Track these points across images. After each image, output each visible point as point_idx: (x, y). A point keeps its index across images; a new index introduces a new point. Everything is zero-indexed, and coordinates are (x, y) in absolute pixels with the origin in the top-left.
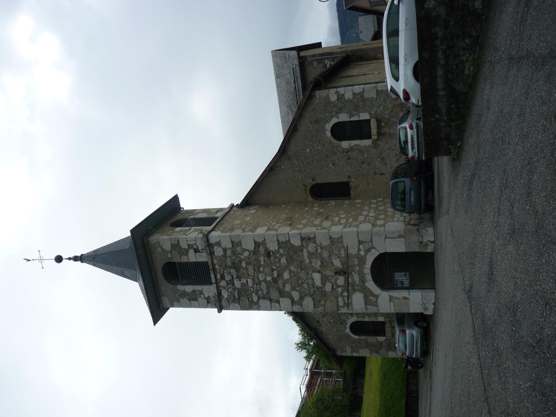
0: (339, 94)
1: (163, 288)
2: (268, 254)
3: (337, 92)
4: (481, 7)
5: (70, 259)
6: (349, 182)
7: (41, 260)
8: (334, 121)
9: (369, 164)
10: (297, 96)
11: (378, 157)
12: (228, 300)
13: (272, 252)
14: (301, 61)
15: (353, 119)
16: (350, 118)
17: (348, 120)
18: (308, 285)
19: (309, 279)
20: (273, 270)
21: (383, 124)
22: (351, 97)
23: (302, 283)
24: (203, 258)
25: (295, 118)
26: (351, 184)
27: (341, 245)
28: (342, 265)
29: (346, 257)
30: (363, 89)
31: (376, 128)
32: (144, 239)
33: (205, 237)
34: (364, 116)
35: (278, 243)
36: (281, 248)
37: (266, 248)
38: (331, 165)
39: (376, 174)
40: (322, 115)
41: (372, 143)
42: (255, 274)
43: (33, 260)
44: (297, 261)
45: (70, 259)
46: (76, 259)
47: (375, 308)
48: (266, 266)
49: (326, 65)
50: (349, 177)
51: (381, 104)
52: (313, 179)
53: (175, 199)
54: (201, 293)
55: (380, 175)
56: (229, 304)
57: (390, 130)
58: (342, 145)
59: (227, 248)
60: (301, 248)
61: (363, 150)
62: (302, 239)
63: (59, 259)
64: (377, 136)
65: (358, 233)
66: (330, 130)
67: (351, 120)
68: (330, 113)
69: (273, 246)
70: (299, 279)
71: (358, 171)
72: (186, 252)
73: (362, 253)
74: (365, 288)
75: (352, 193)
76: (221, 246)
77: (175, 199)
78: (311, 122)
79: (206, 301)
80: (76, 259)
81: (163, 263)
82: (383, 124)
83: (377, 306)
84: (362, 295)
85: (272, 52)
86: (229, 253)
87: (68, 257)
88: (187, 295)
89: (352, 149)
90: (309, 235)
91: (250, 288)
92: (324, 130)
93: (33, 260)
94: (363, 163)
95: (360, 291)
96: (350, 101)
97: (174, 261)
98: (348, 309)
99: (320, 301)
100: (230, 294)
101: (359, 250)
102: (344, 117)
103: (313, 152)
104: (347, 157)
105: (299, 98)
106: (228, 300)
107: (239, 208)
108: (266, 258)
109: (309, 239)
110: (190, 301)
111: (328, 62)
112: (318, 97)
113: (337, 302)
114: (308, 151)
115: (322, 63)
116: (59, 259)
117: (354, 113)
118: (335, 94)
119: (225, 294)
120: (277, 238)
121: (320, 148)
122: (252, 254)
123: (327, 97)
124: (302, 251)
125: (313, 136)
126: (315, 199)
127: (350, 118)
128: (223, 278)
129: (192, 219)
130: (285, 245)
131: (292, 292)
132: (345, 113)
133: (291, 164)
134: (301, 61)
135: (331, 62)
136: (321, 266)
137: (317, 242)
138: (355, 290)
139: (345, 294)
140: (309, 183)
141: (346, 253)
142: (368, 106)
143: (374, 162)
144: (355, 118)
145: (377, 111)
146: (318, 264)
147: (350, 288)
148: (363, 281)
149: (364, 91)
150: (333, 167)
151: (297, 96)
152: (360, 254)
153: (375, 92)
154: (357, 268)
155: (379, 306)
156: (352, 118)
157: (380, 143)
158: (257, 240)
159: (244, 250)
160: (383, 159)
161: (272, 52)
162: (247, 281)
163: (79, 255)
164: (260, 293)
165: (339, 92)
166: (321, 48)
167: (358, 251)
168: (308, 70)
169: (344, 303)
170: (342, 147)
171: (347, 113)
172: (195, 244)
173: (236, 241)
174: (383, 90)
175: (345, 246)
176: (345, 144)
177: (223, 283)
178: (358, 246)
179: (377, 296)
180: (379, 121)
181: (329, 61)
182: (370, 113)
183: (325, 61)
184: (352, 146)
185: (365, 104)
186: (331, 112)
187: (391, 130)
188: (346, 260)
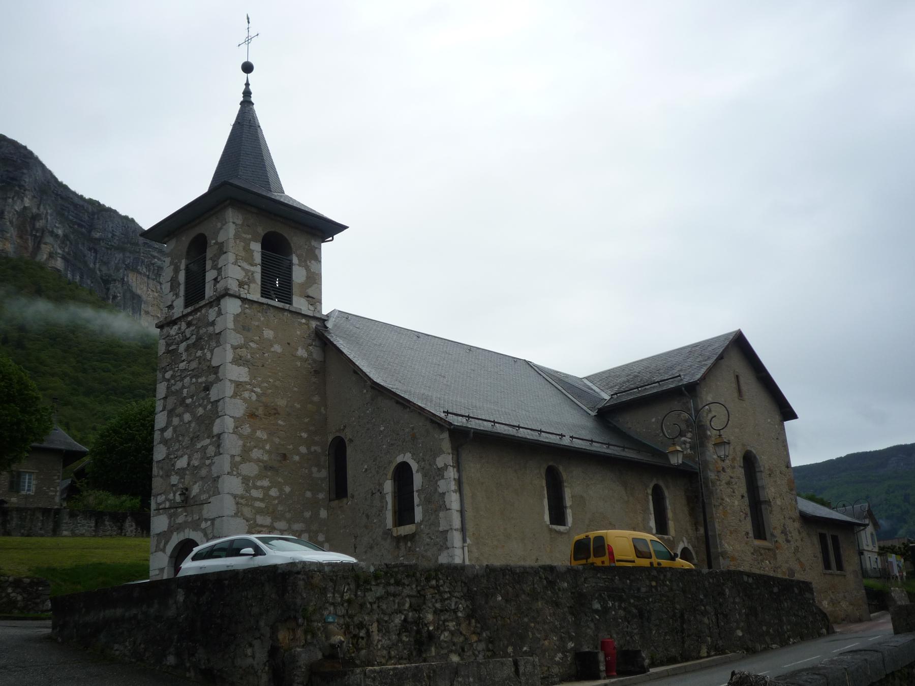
0: (444, 470)
1: (184, 239)
2: (207, 389)
3: (446, 466)
4: (168, 664)
5: (247, 84)
6: (347, 497)
7: (248, 40)
8: (414, 466)
9: (366, 527)
10: (637, 388)
11: (373, 540)
12: (168, 336)
13: (209, 394)
14: (683, 389)
15: (416, 494)
16: (417, 491)
17: (415, 489)
18: (177, 449)
19: (183, 451)
20: (192, 397)
21: (409, 544)
22: (441, 490)
23: (179, 441)
24: (209, 292)
25: (411, 403)
26: (345, 500)
27: (211, 493)
28: (194, 496)
29: (201, 502)
30: (449, 509)
31: (405, 534)
32: (228, 202)
33: (223, 292)
35: (216, 401)
36: (212, 406)
37: (212, 384)
38: (366, 467)
39: (356, 537)
40: (420, 445)
41: (388, 529)
42: (190, 371)
43: (248, 28)
44: (199, 431)
45: (247, 84)
46: (247, 93)
47: (154, 549)
48: (197, 386)
49: (685, 436)
50: (353, 496)
51: (432, 539)
52: (351, 441)
53: (329, 229)
54: (177, 295)
55: (355, 545)
56: (164, 339)
57: (402, 557)
58: (387, 481)
59: (215, 327)
60: (210, 436)
61: (381, 515)
62: (219, 436)
63: (247, 68)
64: (395, 536)
65: (222, 517)
66: (404, 460)
67: (415, 493)
68: (423, 458)
69: (214, 394)
70: (183, 436)
71: (359, 510)
72: (215, 267)
73: (203, 525)
74: (172, 533)
75: (335, 503)
76: (217, 317)
77: (329, 229)
78: (413, 429)
79: (169, 303)
80: (247, 93)
81: (206, 234)
82: (409, 544)
83: (156, 552)
84: (166, 530)
85: (739, 330)
86: (211, 329)
87: (250, 83)
88: (176, 276)
89: (383, 497)
90: (222, 445)
91: (177, 366)
92: (403, 451)
93: (248, 28)
94: (368, 516)
95: (170, 526)
96: (436, 489)
97: (207, 250)
98: (154, 510)
99: (162, 468)
100: (173, 338)
101: (206, 520)
102: (418, 480)
103: (380, 435)
104: (374, 492)
105: (635, 392)
106: (168, 336)
107: (316, 331)
108: (204, 385)
109: (219, 446)
110: (171, 280)
111: (690, 438)
112: (442, 436)
113: (161, 494)
114: (382, 428)
115: (688, 426)
116: (247, 68)
117: (423, 497)
118: (445, 464)
119: (173, 331)
120: (221, 399)
121: (384, 446)
122: (208, 364)
123: (441, 452)
124: (208, 438)
125: (398, 434)
126: (330, 445)
127: (417, 491)
128: (189, 324)
129: (291, 261)
130: (215, 412)
131: (172, 427)
132: (422, 483)
133: (367, 404)
134: (683, 389)
135: (689, 443)
136: (194, 466)
137: (216, 458)
138: (170, 517)
139: (167, 505)
140: (347, 435)
141: (204, 502)
142: (430, 519)
143: (368, 534)
144: (416, 500)
145: (424, 534)
146: (196, 462)
147: (172, 511)
148: (178, 529)
149: (447, 510)
150: (364, 470)
151: (637, 388)
152: (202, 521)
153: (445, 529)
154: (190, 519)
155: (157, 553)
156: (417, 494)
157: (389, 541)
158: (221, 370)
159: (212, 352)
160: (371, 548)
161: (739, 330)
162: (183, 361)
163: (253, 99)
164: (173, 381)
165: (446, 471)
166: (778, 418)
167: (205, 519)
168: (676, 403)
169: (160, 504)
170: (385, 482)
171: (422, 486)
172: (222, 279)
173: (221, 340)
174: (447, 540)
175: (210, 500)
176: (388, 486)
177: (184, 325)
178: (210, 518)
179: (163, 550)
180: (411, 537)
181: (690, 440)
182: (421, 523)
183: (691, 432)
184: (386, 498)
185: (432, 514)
186: (424, 461)
187: (402, 558)
188: (198, 503)
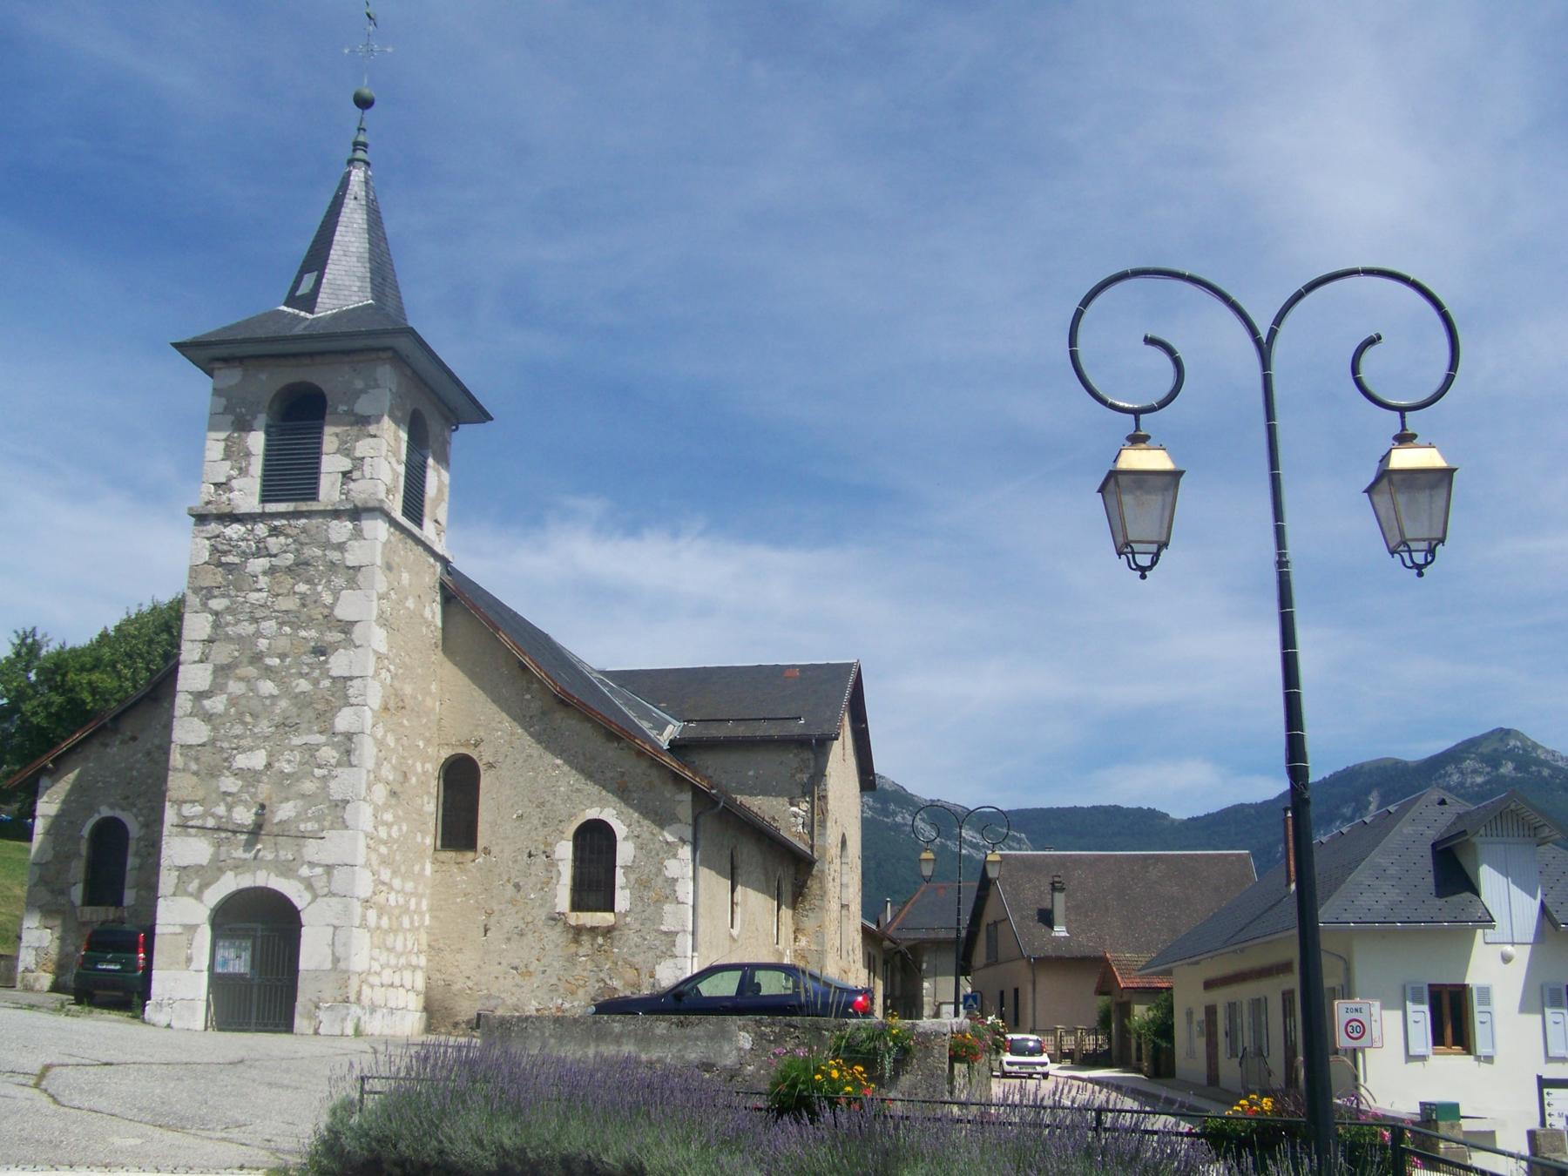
1: (263, 377)
2: (320, 651)
6: (476, 851)
8: (620, 829)
9: (513, 902)
12: (218, 536)
13: (326, 662)
15: (619, 872)
17: (619, 862)
20: (282, 656)
21: (600, 940)
23: (245, 724)
24: (329, 490)
26: (470, 855)
27: (327, 824)
28: (281, 822)
29: (300, 835)
30: (683, 903)
32: (390, 354)
34: (622, 900)
35: (344, 678)
37: (335, 647)
39: (490, 915)
42: (278, 612)
47: (172, 890)
49: (798, 806)
50: (487, 851)
51: (645, 939)
52: (491, 766)
54: (243, 472)
56: (208, 539)
58: (563, 842)
62: (349, 736)
67: (618, 869)
69: (339, 664)
72: (346, 452)
74: (221, 871)
76: (350, 540)
78: (623, 774)
82: (600, 940)
83: (174, 895)
84: (205, 863)
86: (334, 556)
89: (551, 863)
90: (357, 753)
91: (243, 594)
94: (517, 886)
95: (215, 859)
96: (660, 871)
98: (172, 825)
99: (197, 759)
101: (312, 865)
106: (218, 536)
108: (313, 644)
109: (348, 752)
110: (225, 440)
112: (678, 797)
113: (193, 802)
117: (632, 877)
119: (235, 531)
121: (562, 789)
122: (326, 611)
128: (275, 532)
131: (225, 696)
133: (531, 717)
136: (282, 772)
137: (339, 770)
138: (218, 845)
140: (482, 756)
141: (307, 835)
148: (237, 867)
152: (302, 865)
153: (672, 929)
157: (559, 929)
162: (260, 590)
164: (229, 618)
168: (791, 756)
171: (633, 862)
172: (363, 477)
173: (360, 577)
174: (674, 946)
176: (565, 851)
179: (198, 895)
180: (608, 931)
182: (626, 915)
183: (807, 802)
